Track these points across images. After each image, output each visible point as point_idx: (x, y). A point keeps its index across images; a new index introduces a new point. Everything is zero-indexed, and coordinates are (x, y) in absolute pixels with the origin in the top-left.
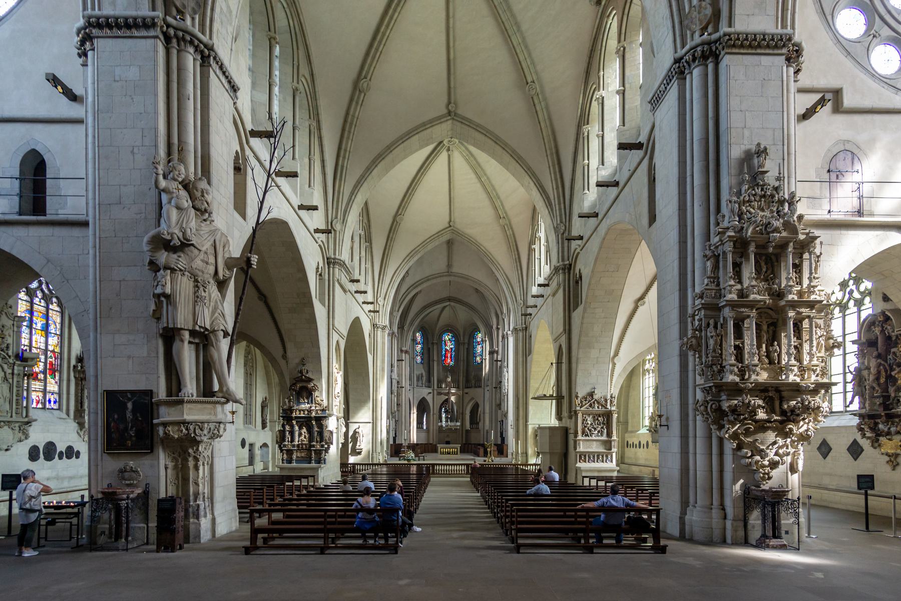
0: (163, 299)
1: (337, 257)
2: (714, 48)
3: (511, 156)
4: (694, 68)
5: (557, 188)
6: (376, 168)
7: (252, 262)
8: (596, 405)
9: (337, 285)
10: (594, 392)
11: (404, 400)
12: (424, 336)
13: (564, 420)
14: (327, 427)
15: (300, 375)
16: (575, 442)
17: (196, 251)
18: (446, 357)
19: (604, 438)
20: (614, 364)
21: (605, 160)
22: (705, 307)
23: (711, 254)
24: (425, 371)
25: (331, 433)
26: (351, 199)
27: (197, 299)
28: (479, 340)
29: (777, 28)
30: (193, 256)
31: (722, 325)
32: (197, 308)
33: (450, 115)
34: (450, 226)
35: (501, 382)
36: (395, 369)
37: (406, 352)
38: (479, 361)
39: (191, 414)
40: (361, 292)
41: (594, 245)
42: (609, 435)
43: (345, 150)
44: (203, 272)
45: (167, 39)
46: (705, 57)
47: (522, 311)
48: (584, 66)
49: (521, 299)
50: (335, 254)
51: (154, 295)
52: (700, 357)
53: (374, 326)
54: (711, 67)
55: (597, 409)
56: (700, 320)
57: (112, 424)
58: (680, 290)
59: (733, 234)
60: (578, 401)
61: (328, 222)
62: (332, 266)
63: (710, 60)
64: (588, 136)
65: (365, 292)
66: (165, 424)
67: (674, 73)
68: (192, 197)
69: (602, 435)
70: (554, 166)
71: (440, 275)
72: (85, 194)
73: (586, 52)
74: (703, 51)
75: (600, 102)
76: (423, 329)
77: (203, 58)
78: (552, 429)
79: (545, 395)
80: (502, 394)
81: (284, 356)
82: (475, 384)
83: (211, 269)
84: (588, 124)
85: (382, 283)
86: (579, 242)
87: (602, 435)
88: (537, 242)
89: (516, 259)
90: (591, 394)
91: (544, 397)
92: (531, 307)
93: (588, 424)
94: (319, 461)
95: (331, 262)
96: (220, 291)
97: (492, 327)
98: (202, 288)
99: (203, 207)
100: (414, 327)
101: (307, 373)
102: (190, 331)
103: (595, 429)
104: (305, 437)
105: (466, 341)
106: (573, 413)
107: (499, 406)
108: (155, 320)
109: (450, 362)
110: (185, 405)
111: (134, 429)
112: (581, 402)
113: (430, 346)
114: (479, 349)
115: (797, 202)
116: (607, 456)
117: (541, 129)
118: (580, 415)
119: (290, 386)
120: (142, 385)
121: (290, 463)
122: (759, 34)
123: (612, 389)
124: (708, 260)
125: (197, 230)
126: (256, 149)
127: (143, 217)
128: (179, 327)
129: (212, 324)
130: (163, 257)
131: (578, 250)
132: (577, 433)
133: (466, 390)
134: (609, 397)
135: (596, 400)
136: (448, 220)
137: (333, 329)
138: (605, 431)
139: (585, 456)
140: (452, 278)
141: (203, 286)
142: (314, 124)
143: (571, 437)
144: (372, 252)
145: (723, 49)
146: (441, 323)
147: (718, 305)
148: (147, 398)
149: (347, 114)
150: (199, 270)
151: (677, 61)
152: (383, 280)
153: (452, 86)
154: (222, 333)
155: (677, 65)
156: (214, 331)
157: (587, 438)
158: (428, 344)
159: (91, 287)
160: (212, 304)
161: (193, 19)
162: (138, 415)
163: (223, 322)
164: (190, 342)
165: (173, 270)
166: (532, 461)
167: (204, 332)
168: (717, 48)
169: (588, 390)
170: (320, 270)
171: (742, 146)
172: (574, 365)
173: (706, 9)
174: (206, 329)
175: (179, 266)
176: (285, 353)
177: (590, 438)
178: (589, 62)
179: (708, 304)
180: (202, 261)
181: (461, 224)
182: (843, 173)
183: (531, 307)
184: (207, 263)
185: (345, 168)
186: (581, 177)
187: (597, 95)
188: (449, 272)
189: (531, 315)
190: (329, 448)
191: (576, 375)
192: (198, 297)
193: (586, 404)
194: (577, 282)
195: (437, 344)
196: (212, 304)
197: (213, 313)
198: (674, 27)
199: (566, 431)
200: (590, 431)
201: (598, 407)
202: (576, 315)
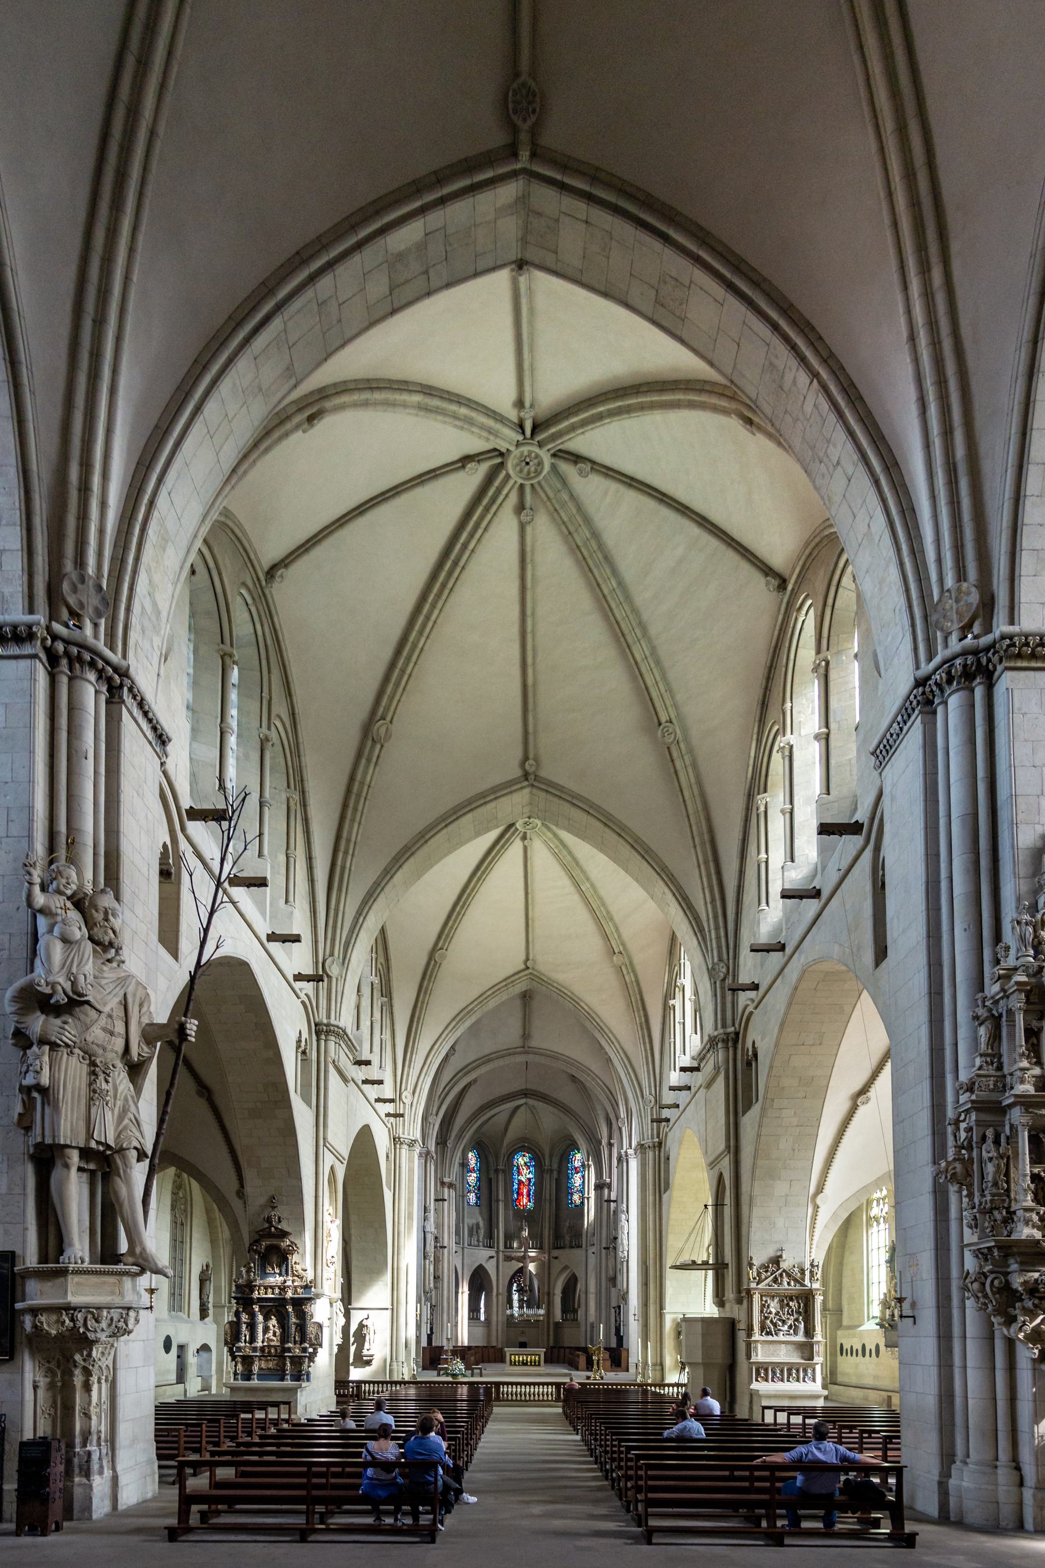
0: (35, 1094)
1: (333, 1021)
3: (632, 846)
4: (950, 695)
5: (713, 901)
6: (401, 870)
7: (188, 1032)
8: (785, 1280)
9: (331, 1069)
10: (781, 1256)
11: (446, 1270)
12: (482, 1157)
13: (727, 1305)
14: (312, 1316)
15: (267, 1225)
16: (749, 1345)
17: (93, 1013)
18: (520, 1194)
19: (800, 1338)
20: (816, 1207)
21: (796, 853)
22: (978, 1106)
23: (986, 1014)
24: (483, 1219)
25: (320, 1326)
26: (357, 922)
27: (93, 1094)
28: (577, 1164)
30: (88, 1021)
31: (1008, 1138)
32: (93, 1110)
33: (527, 779)
34: (528, 968)
35: (616, 1238)
36: (432, 1215)
37: (451, 1186)
38: (578, 1202)
40: (373, 1082)
41: (778, 1000)
42: (809, 1332)
44: (104, 1049)
46: (968, 675)
47: (652, 1115)
48: (757, 693)
49: (650, 1094)
50: (329, 1017)
51: (22, 1088)
52: (971, 1195)
53: (396, 1140)
54: (979, 692)
55: (787, 1287)
56: (969, 1130)
58: (932, 1077)
60: (753, 1273)
61: (317, 963)
62: (323, 1037)
63: (978, 680)
64: (766, 812)
65: (380, 1082)
67: (915, 703)
68: (89, 922)
69: (796, 1333)
70: (706, 863)
71: (509, 1053)
73: (761, 671)
74: (965, 666)
75: (787, 753)
76: (480, 1146)
78: (706, 1321)
79: (694, 1262)
80: (618, 1260)
81: (241, 1194)
82: (571, 1242)
83: (119, 1044)
84: (765, 791)
85: (409, 1067)
86: (752, 994)
87: (796, 1333)
88: (679, 995)
89: (641, 1024)
90: (776, 1261)
91: (692, 1266)
92: (669, 1107)
93: (771, 1313)
94: (300, 1376)
95: (321, 1031)
96: (132, 1081)
97: (600, 1143)
98: (102, 1077)
99: (107, 939)
100: (465, 1141)
101: (280, 1221)
102: (81, 1149)
103: (784, 1322)
104: (274, 1334)
105: (555, 1166)
106: (744, 1294)
107: (613, 1280)
108: (23, 1132)
109: (527, 1203)
110: (70, 1277)
112: (759, 1274)
113: (492, 1175)
114: (577, 1180)
116: (805, 1371)
117: (684, 801)
118: (756, 1298)
119: (251, 1245)
121: (249, 1379)
123: (813, 1250)
124: (980, 1025)
128: (62, 1142)
129: (118, 1137)
130: (38, 1023)
131: (750, 1009)
132: (752, 1330)
133: (555, 1253)
134: (807, 1266)
135: (784, 1271)
136: (523, 957)
137: (325, 1145)
138: (802, 1326)
139: (766, 1370)
140: (530, 1058)
141: (104, 1073)
143: (742, 1336)
144: (392, 1013)
145: (1001, 661)
146: (511, 1135)
147: (1000, 1102)
148: (6, 1265)
150: (97, 1045)
151: (920, 683)
153: (531, 729)
154: (134, 1153)
155: (921, 689)
156: (121, 1150)
157: (770, 1338)
158: (488, 1171)
160: (119, 1103)
163: (138, 1134)
164: (80, 1169)
165: (54, 1046)
166: (672, 1377)
167: (104, 1151)
168: (989, 660)
169: (771, 1252)
170: (303, 1044)
171: (1037, 826)
172: (745, 1209)
173: (968, 594)
174: (108, 1147)
175: (64, 1039)
176: (242, 1186)
177: (775, 1338)
178: (766, 688)
179: (982, 1102)
180: (104, 1029)
181: (546, 963)
183: (669, 1107)
184: (112, 1034)
186: (755, 882)
187: (781, 742)
188: (525, 1048)
189: (668, 1120)
190: (315, 1353)
191: (749, 1227)
192: (95, 1091)
193: (766, 1278)
194: (749, 1064)
195: (504, 1171)
196: (119, 1103)
197: (121, 1118)
198: (913, 625)
199: (731, 1325)
200: (775, 1325)
201: (789, 1284)
202: (749, 1121)
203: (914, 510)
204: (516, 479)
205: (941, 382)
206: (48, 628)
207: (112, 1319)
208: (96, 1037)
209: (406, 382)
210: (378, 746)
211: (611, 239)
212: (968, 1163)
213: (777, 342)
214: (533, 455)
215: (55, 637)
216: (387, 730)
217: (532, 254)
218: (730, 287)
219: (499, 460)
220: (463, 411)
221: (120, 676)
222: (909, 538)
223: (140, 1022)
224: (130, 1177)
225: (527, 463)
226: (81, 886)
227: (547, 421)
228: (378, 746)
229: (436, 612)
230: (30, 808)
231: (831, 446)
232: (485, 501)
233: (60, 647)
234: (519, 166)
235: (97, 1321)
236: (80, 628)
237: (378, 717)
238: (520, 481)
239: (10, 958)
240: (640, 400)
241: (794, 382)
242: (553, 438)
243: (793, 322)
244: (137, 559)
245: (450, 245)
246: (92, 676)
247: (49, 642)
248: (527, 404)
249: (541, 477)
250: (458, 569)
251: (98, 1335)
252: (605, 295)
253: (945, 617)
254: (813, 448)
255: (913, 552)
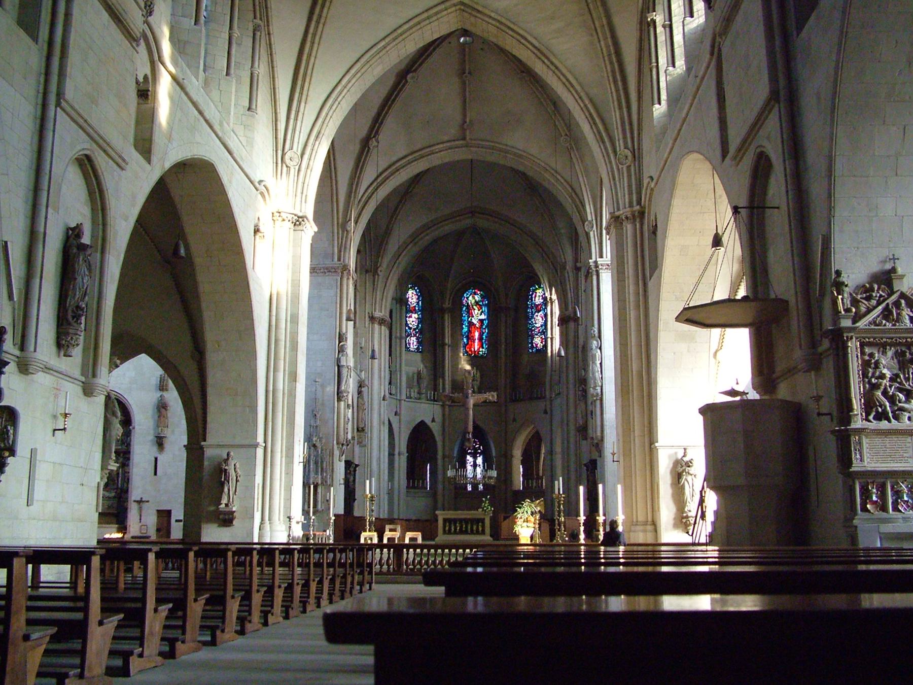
10: (893, 270)
90: (886, 278)
93: (882, 376)
112: (855, 302)
118: (853, 346)
135: (903, 296)
139: (882, 489)
157: (884, 424)
172: (816, 188)
193: (869, 311)
200: (892, 400)
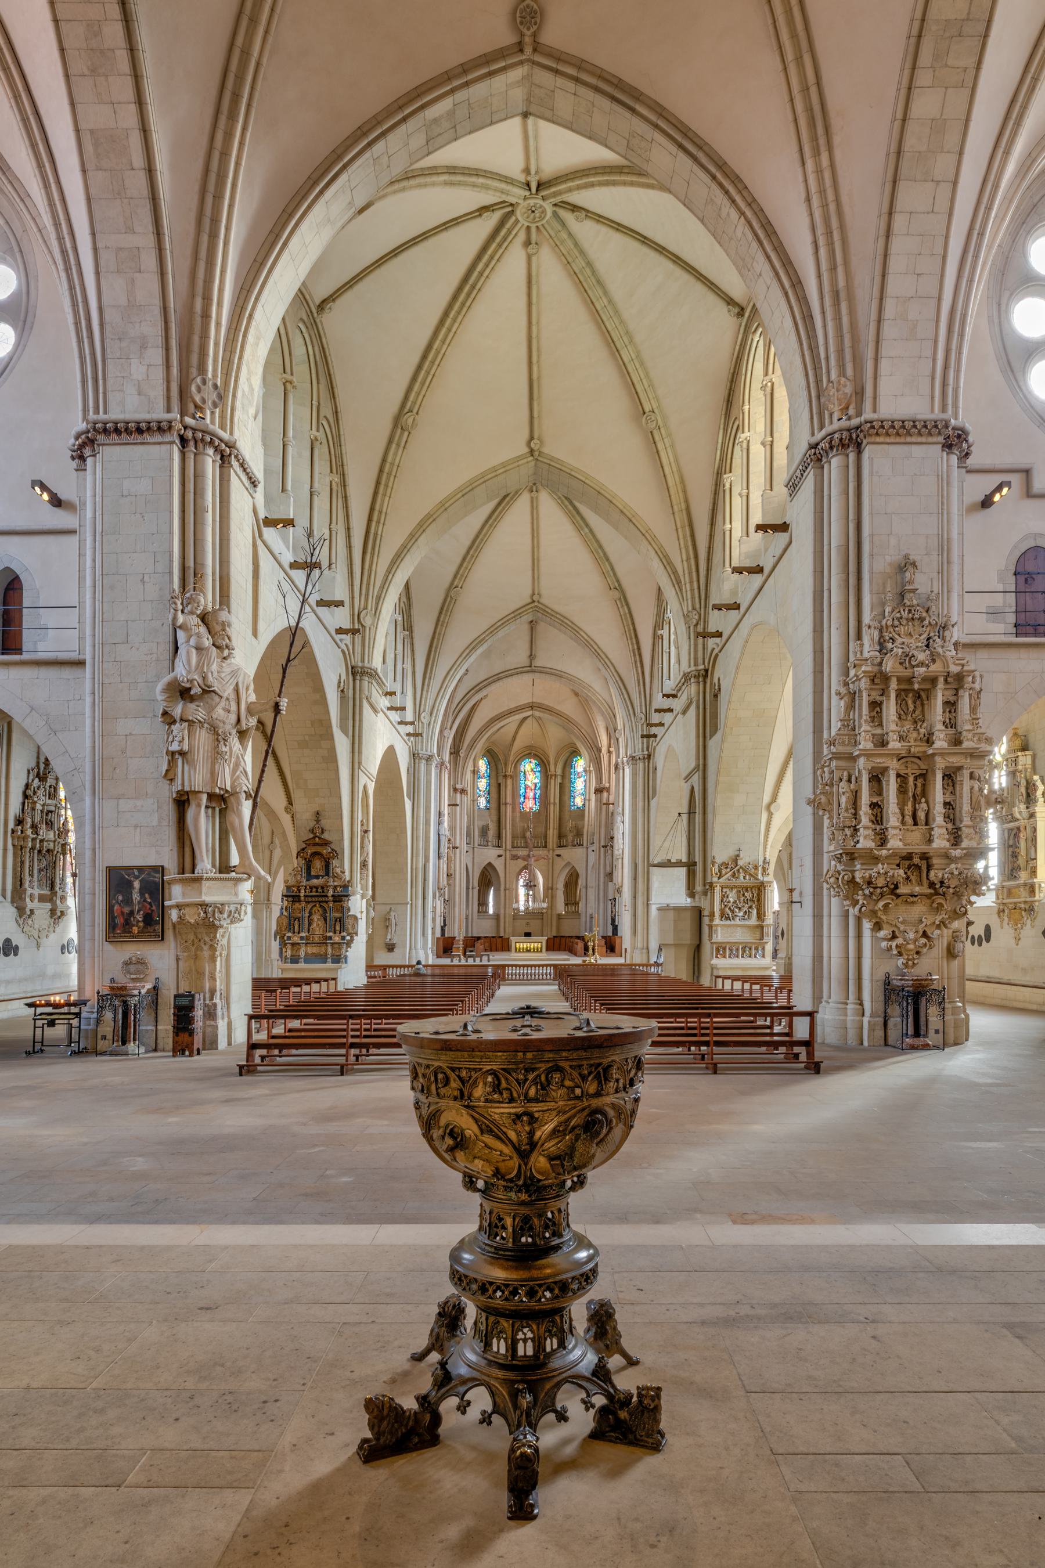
0: (177, 756)
2: (854, 436)
4: (832, 457)
6: (424, 534)
7: (281, 708)
29: (932, 411)
31: (856, 778)
32: (217, 766)
39: (211, 894)
43: (380, 512)
45: (183, 441)
46: (843, 445)
54: (852, 456)
57: (115, 908)
59: (869, 669)
63: (851, 449)
66: (179, 907)
72: (77, 627)
74: (841, 440)
77: (222, 457)
83: (233, 718)
96: (241, 743)
99: (224, 643)
102: (208, 793)
108: (168, 782)
110: (204, 882)
111: (142, 912)
115: (953, 626)
120: (152, 861)
122: (909, 421)
124: (841, 699)
125: (218, 672)
126: (270, 542)
127: (154, 659)
142: (336, 479)
145: (865, 437)
147: (852, 754)
148: (157, 875)
149: (384, 461)
152: (429, 685)
154: (244, 795)
155: (813, 450)
159: (88, 743)
161: (213, 413)
162: (147, 895)
163: (246, 782)
168: (858, 436)
171: (886, 557)
173: (845, 386)
174: (227, 791)
182: (1034, 576)
185: (379, 537)
192: (218, 753)
198: (810, 402)
203: (812, 316)
204: (523, 222)
205: (829, 233)
206: (181, 422)
207: (230, 912)
208: (218, 715)
209: (435, 167)
210: (406, 434)
211: (593, 106)
212: (829, 795)
213: (714, 187)
214: (538, 206)
215: (185, 428)
216: (414, 420)
217: (533, 109)
218: (681, 146)
219: (510, 209)
220: (481, 180)
221: (229, 447)
222: (809, 337)
223: (246, 702)
224: (241, 811)
225: (533, 212)
226: (206, 606)
227: (549, 181)
228: (406, 434)
229: (456, 325)
230: (171, 553)
231: (755, 263)
232: (498, 239)
233: (189, 434)
234: (524, 57)
235: (221, 913)
236: (203, 419)
237: (406, 410)
238: (527, 224)
239: (157, 660)
240: (623, 178)
241: (728, 214)
242: (555, 194)
243: (726, 175)
244: (240, 358)
245: (472, 109)
246: (210, 451)
247: (183, 431)
248: (533, 172)
249: (544, 221)
250: (475, 292)
251: (222, 923)
252: (590, 138)
253: (829, 401)
254: (743, 260)
255: (811, 348)
